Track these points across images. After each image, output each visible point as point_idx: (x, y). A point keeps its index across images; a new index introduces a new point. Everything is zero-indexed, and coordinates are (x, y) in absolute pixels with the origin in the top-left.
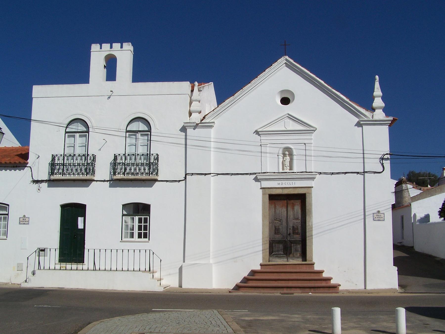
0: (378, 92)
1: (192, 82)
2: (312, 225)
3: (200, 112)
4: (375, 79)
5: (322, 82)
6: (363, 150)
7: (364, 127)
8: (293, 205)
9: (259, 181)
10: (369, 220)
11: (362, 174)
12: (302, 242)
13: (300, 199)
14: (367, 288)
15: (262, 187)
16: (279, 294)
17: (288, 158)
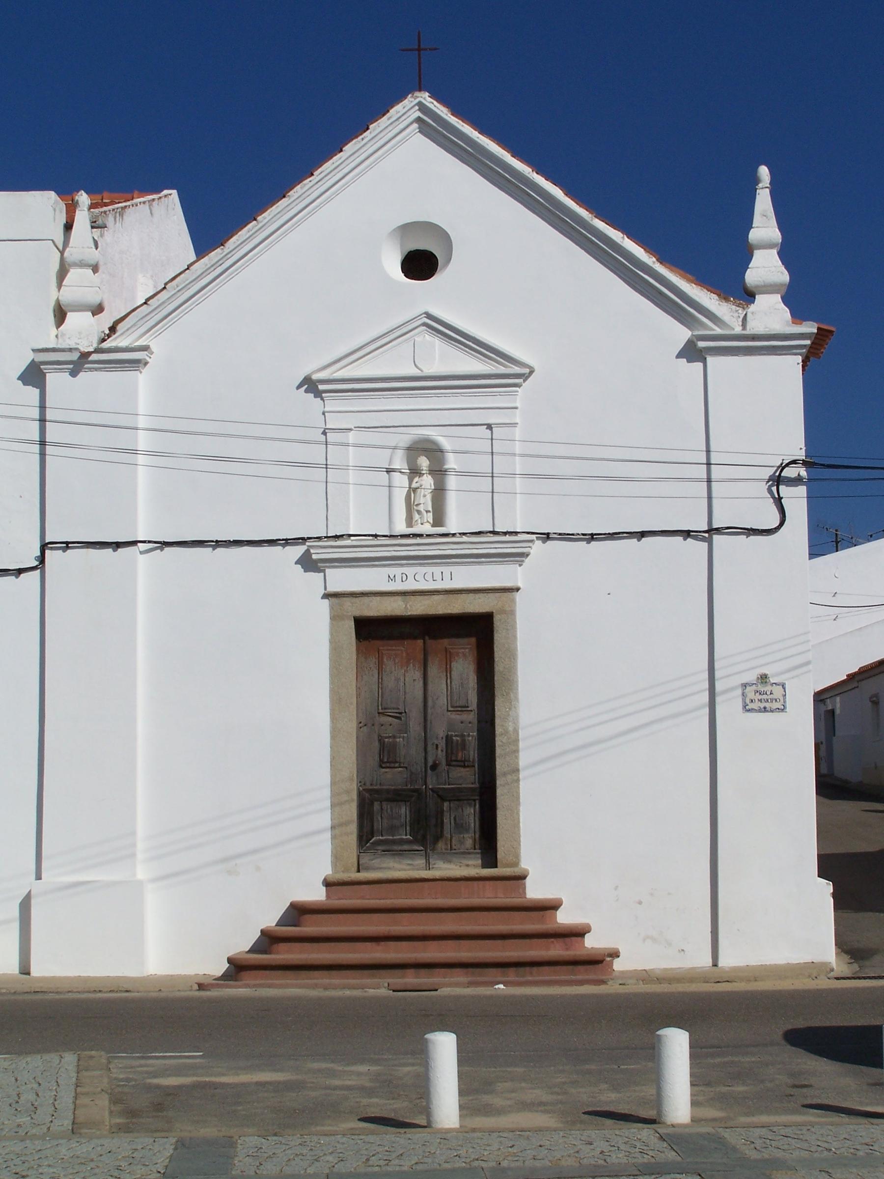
0: (765, 227)
1: (66, 191)
2: (516, 731)
3: (97, 310)
4: (756, 180)
5: (557, 192)
6: (708, 451)
7: (710, 359)
8: (448, 658)
9: (318, 570)
10: (729, 708)
11: (703, 539)
12: (481, 795)
13: (472, 634)
14: (722, 963)
15: (331, 589)
16: (383, 992)
17: (427, 482)
